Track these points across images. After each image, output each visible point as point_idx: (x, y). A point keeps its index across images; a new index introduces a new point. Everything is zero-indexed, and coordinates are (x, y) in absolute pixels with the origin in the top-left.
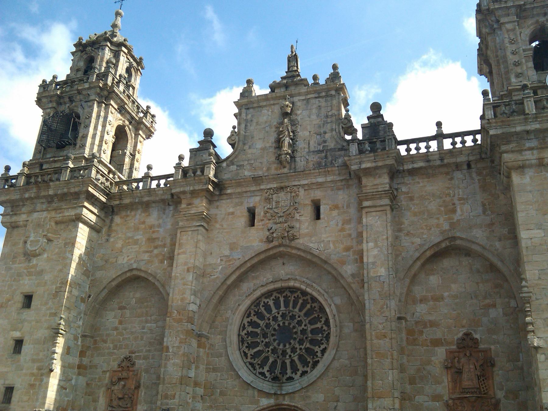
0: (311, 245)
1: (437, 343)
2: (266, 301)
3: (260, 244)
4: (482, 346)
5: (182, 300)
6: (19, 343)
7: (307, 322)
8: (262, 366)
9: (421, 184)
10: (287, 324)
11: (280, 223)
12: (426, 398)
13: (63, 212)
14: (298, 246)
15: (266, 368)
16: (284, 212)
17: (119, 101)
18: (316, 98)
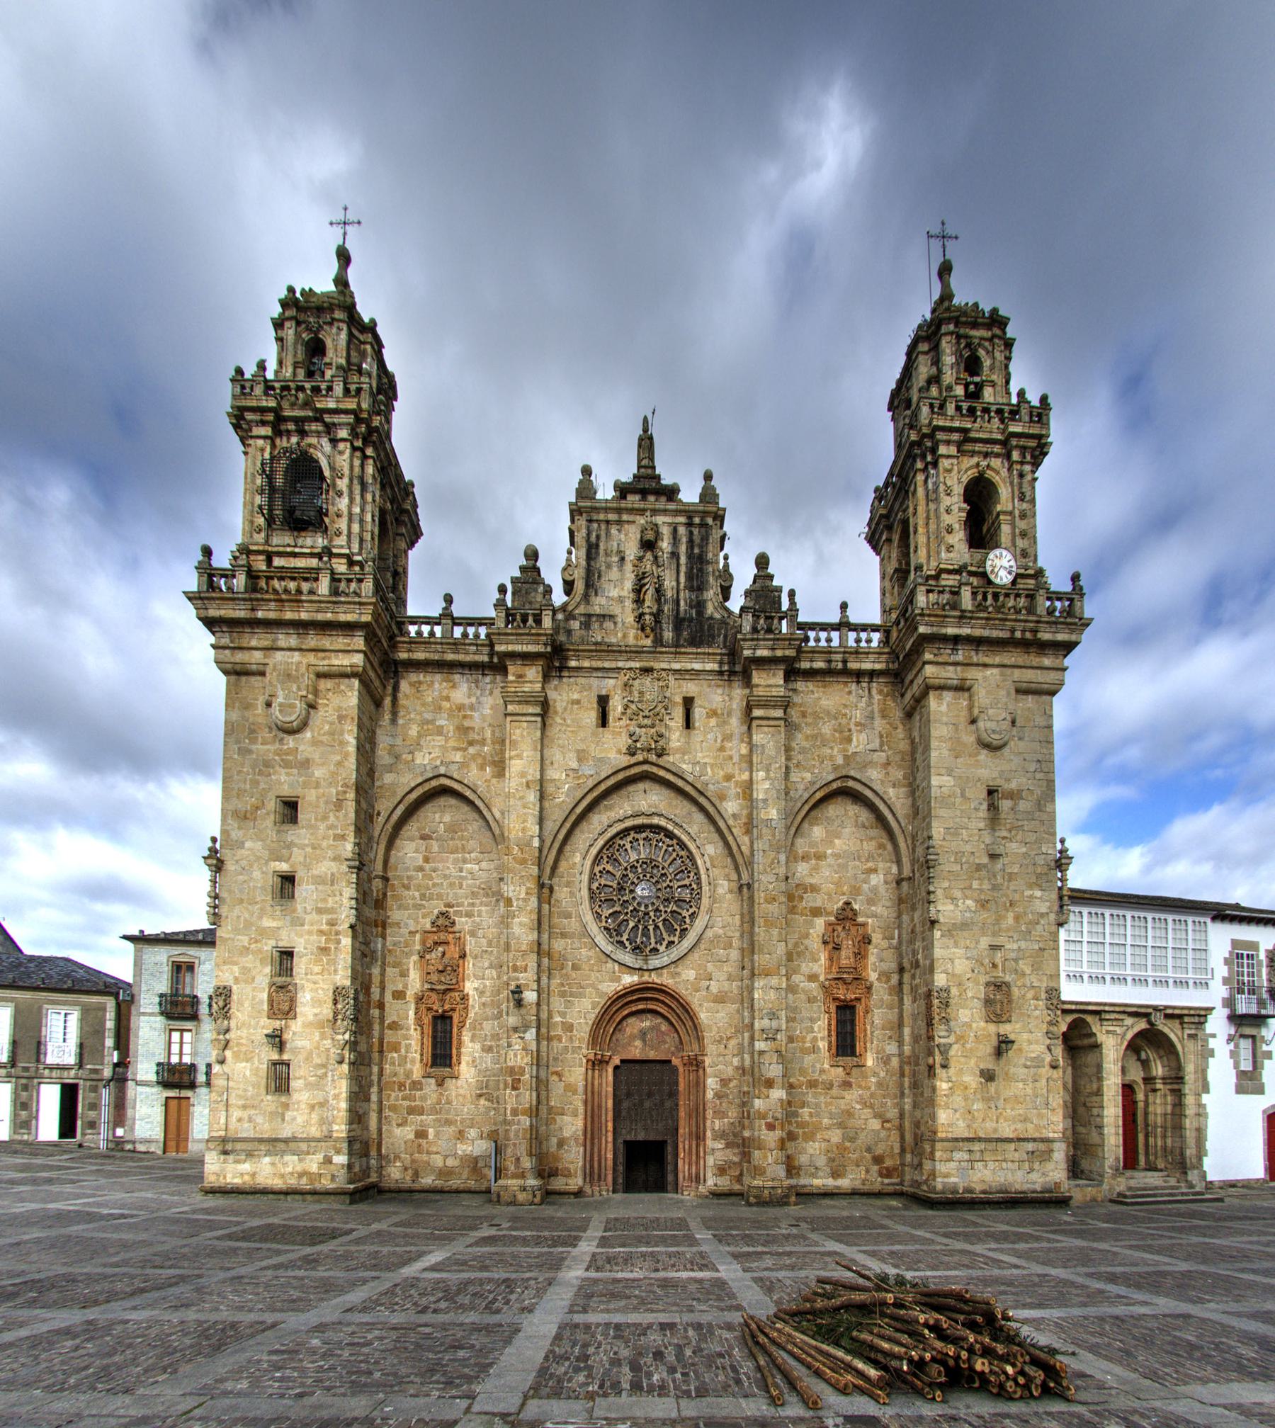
0: (684, 766)
1: (816, 912)
4: (860, 919)
6: (288, 881)
11: (645, 726)
12: (803, 978)
13: (329, 658)
14: (667, 766)
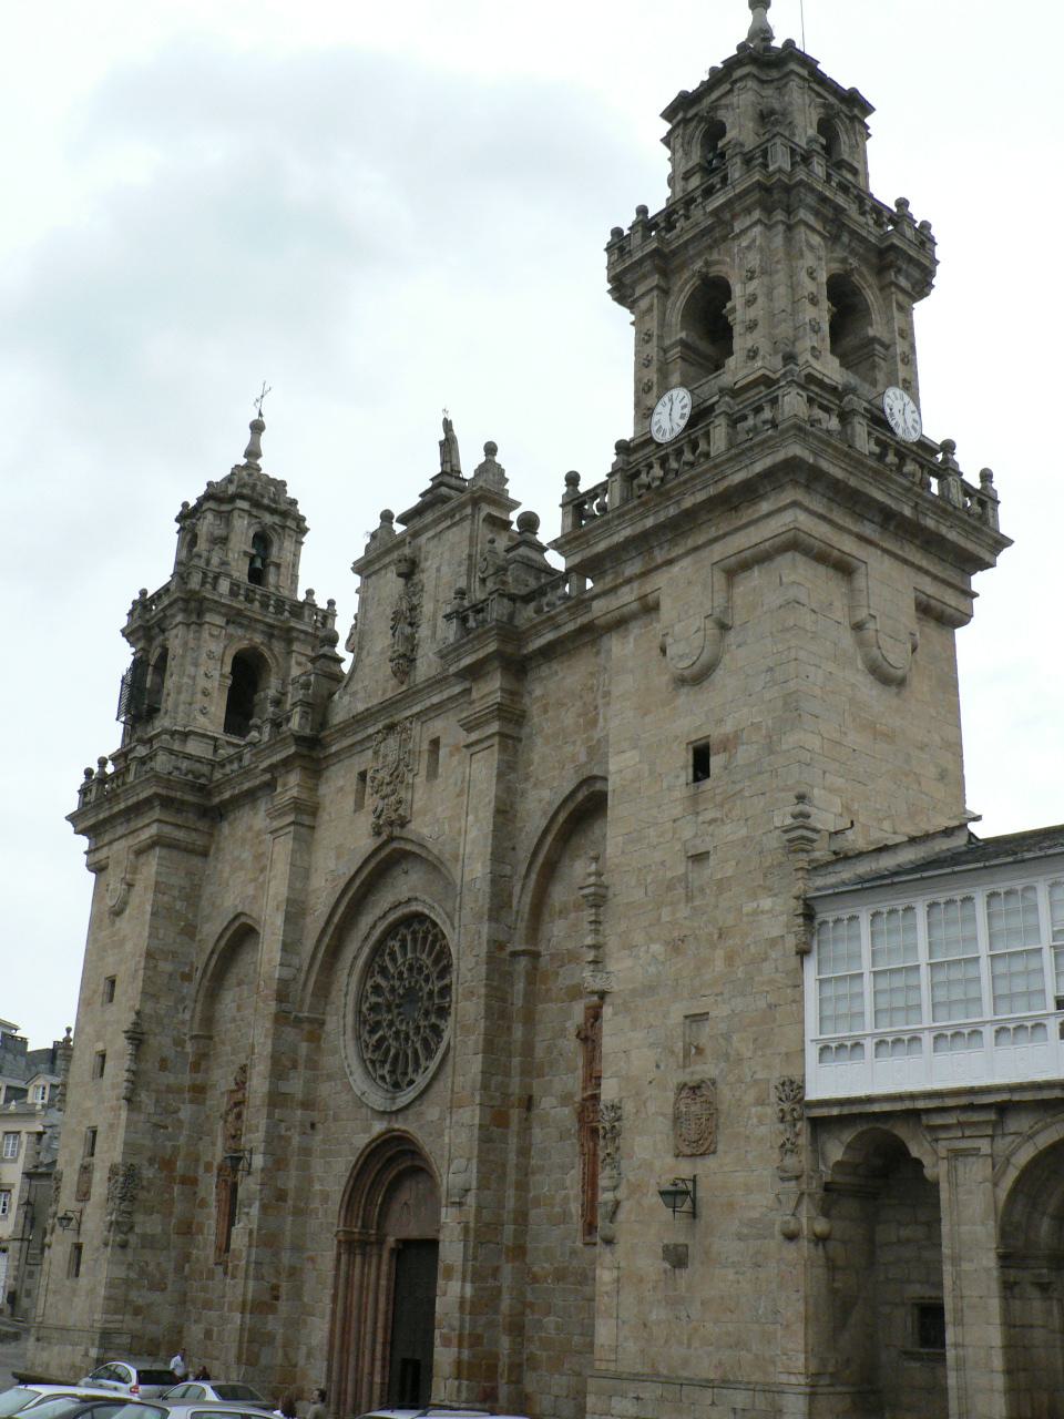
2: (391, 943)
3: (369, 841)
5: (270, 961)
7: (435, 975)
8: (383, 1063)
9: (561, 675)
10: (413, 984)
13: (138, 836)
15: (387, 1067)
16: (392, 774)
17: (223, 610)
18: (449, 528)
